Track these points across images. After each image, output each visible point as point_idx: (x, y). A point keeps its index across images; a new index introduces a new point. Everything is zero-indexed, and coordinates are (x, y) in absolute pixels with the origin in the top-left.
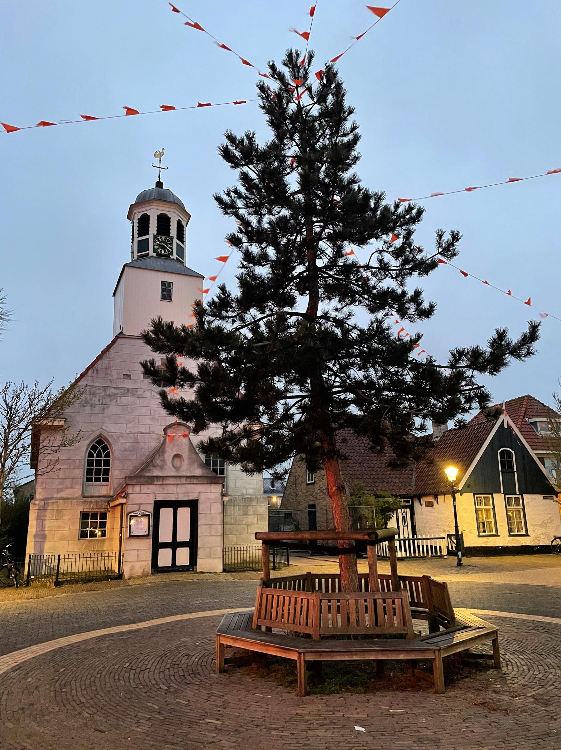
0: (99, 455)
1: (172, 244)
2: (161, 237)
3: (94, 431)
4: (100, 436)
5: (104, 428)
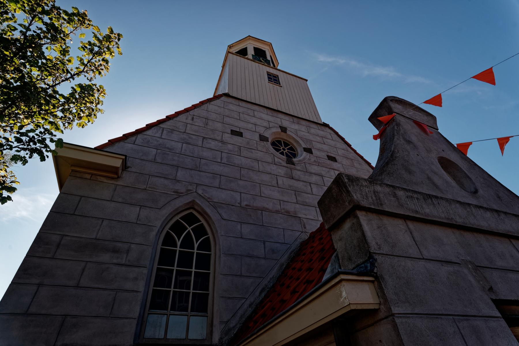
0: (188, 243)
3: (178, 194)
4: (192, 205)
5: (200, 192)
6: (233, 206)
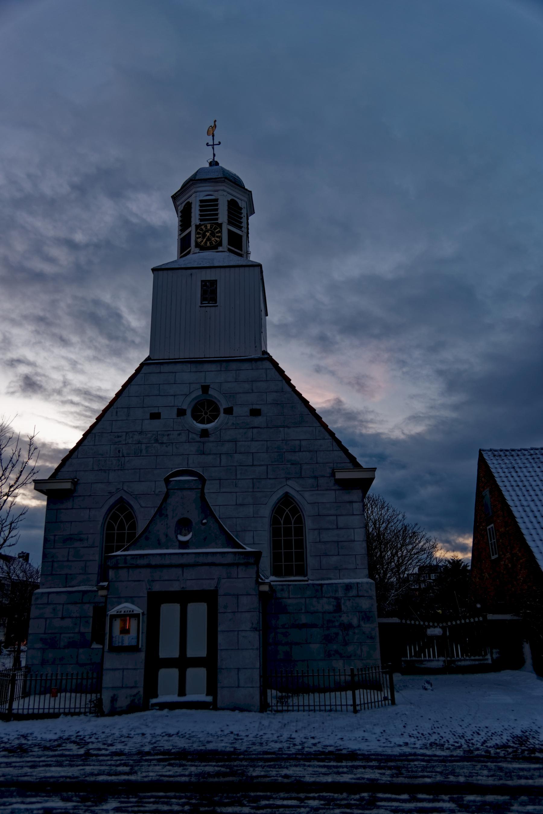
1: (220, 232)
2: (206, 227)
3: (111, 494)
4: (121, 499)
5: (125, 488)
6: (149, 494)
